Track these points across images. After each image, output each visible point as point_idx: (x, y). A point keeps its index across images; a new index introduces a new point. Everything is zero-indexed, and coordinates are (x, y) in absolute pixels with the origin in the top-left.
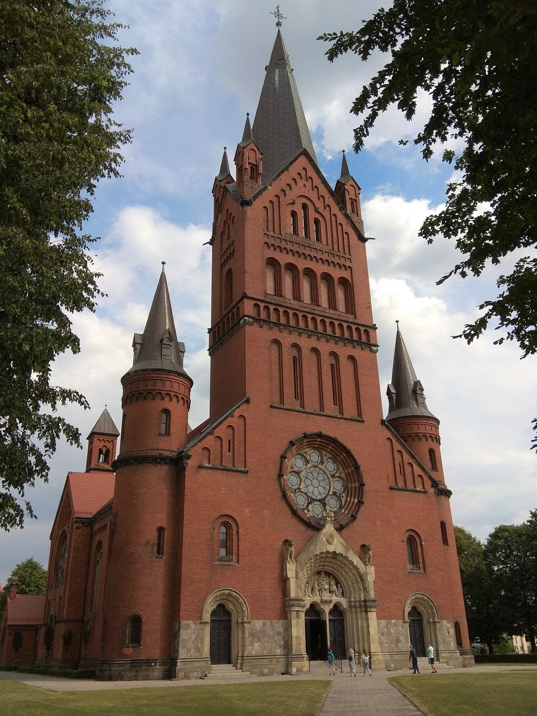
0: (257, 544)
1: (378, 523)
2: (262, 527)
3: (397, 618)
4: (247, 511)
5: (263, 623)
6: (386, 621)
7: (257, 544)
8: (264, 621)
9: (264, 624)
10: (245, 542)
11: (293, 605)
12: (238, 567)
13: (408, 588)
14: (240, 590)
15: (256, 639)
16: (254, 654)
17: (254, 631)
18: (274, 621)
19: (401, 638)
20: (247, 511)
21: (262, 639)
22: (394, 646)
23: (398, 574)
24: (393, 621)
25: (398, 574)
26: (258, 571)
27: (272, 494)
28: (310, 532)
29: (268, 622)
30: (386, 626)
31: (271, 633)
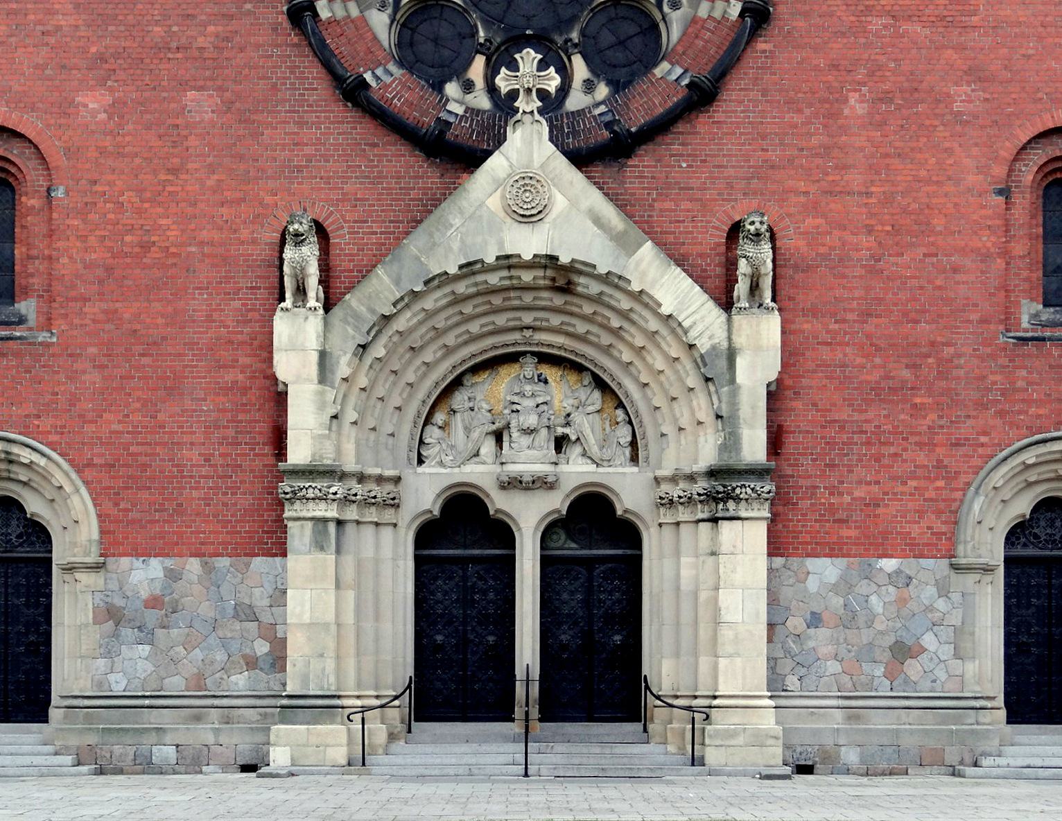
0: (146, 247)
1: (856, 106)
2: (174, 171)
3: (915, 550)
4: (93, 103)
5: (165, 569)
6: (842, 562)
7: (146, 247)
8: (169, 562)
9: (173, 576)
10: (84, 238)
11: (295, 497)
12: (47, 345)
13: (1001, 414)
14: (53, 438)
15: (127, 633)
16: (118, 689)
17: (118, 602)
18: (223, 562)
19: (928, 640)
20: (93, 103)
21: (160, 633)
22: (879, 671)
23: (948, 351)
24: (889, 564)
25: (948, 351)
26: (146, 361)
27: (231, 17)
28: (425, 174)
29: (193, 566)
30: (844, 586)
31: (206, 610)
